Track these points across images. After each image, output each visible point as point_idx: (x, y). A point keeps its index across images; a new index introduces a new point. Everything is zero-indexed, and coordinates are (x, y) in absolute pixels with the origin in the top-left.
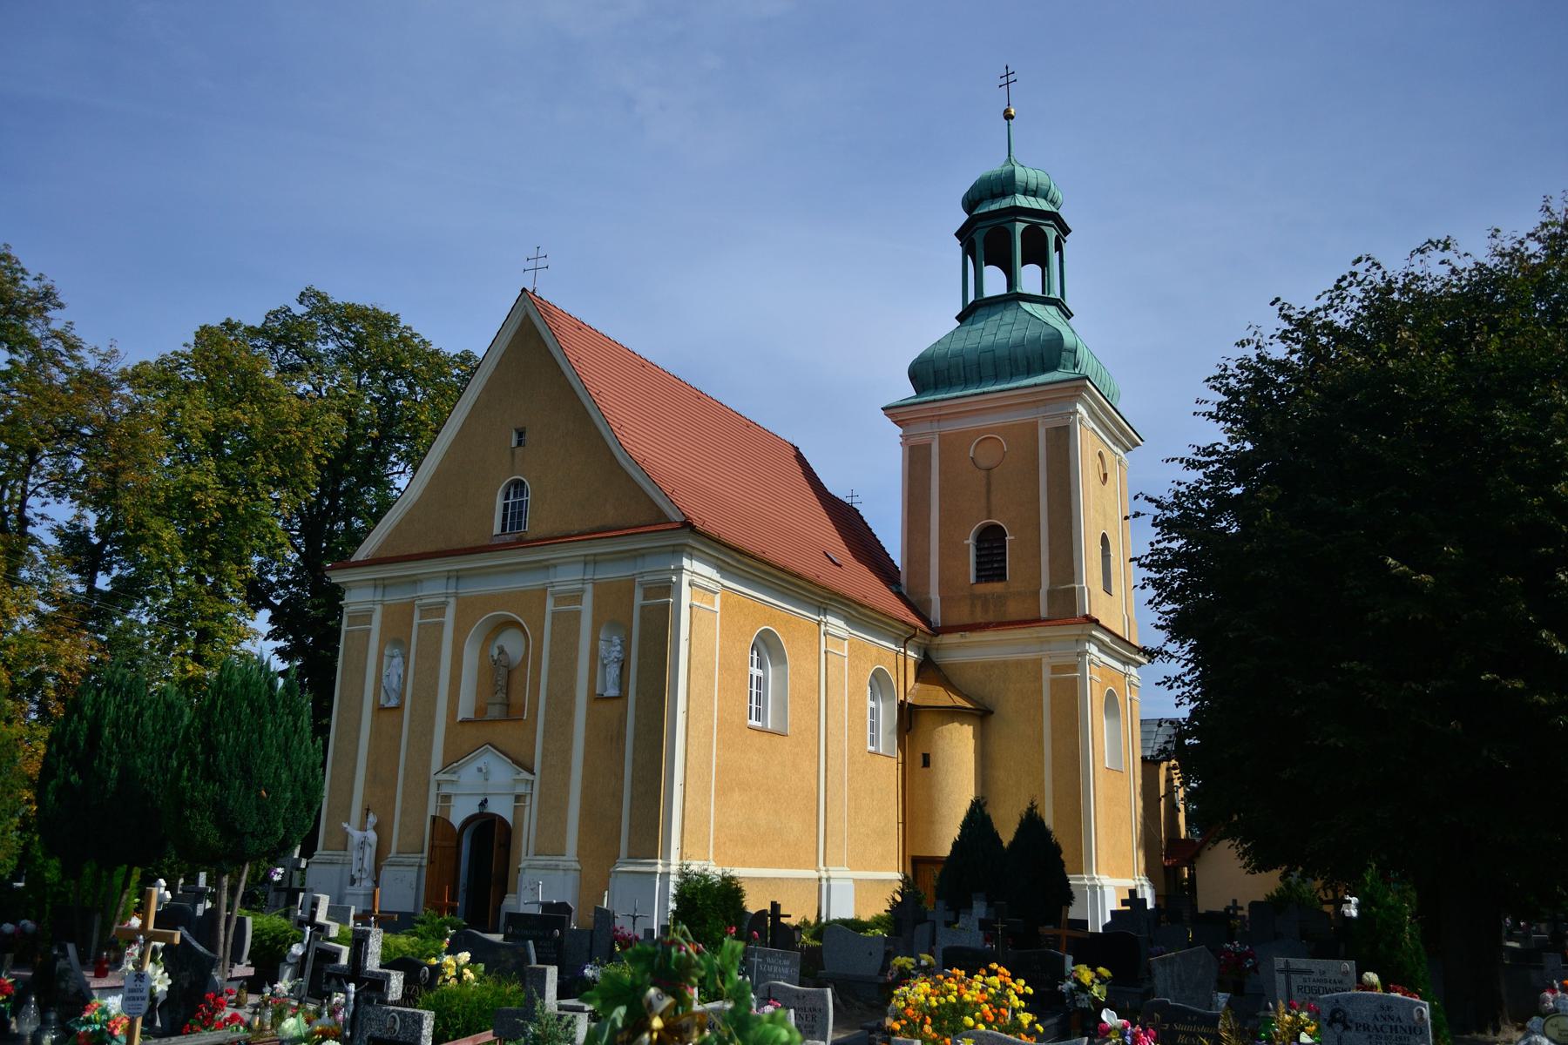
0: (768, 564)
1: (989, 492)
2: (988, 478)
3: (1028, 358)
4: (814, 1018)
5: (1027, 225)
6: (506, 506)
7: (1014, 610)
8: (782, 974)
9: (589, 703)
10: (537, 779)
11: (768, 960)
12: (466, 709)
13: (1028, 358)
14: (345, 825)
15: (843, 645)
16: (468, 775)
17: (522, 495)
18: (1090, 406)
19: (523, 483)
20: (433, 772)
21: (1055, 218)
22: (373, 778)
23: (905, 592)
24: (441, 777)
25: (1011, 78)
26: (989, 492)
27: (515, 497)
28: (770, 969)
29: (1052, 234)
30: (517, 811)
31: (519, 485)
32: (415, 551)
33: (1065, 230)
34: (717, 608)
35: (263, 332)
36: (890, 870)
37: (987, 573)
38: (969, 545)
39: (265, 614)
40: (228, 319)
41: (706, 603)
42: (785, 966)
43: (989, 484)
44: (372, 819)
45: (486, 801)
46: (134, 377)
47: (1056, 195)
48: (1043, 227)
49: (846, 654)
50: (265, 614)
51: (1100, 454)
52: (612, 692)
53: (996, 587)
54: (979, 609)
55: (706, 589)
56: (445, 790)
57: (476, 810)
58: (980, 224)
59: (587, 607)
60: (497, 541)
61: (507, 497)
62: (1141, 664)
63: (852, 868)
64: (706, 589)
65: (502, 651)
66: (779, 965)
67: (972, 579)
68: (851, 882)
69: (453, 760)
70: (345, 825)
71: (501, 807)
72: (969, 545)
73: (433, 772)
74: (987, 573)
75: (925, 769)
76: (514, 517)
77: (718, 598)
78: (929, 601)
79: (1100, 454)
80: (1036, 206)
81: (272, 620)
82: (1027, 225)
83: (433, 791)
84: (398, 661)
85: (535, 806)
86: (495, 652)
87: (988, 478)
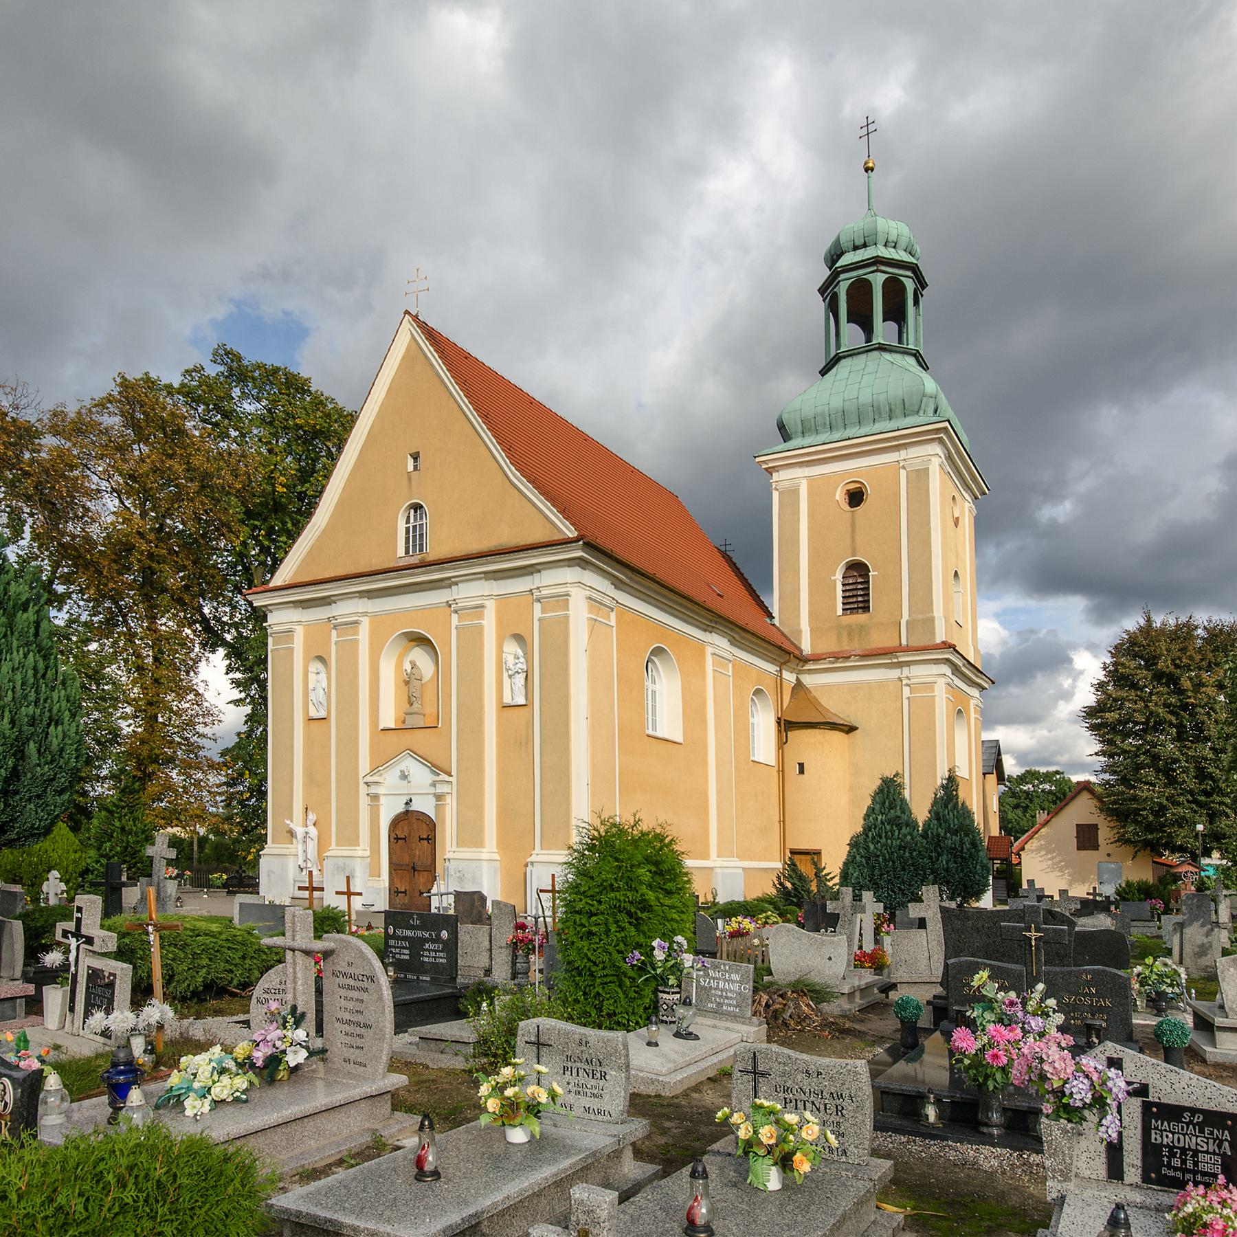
0: (658, 583)
1: (853, 531)
2: (853, 516)
3: (890, 404)
4: (839, 1110)
5: (887, 276)
6: (407, 530)
7: (879, 640)
8: (731, 991)
9: (498, 713)
10: (453, 779)
11: (711, 973)
12: (388, 718)
13: (890, 404)
14: (288, 822)
15: (727, 665)
16: (390, 779)
17: (421, 518)
18: (947, 449)
19: (421, 507)
20: (361, 775)
21: (914, 269)
22: (310, 779)
23: (778, 624)
24: (368, 779)
25: (871, 128)
26: (853, 531)
27: (415, 520)
28: (714, 984)
29: (910, 285)
30: (439, 808)
31: (417, 507)
32: (328, 576)
33: (921, 283)
34: (613, 623)
35: (185, 391)
36: (773, 860)
37: (852, 606)
38: (835, 581)
39: (221, 652)
40: (146, 374)
41: (602, 617)
42: (733, 982)
43: (853, 524)
44: (312, 817)
45: (411, 800)
46: (59, 424)
47: (915, 247)
48: (901, 278)
49: (730, 674)
50: (221, 652)
51: (954, 498)
52: (522, 701)
53: (861, 618)
54: (845, 638)
55: (601, 604)
56: (373, 790)
57: (401, 808)
58: (842, 276)
59: (489, 622)
60: (401, 563)
61: (408, 521)
62: (984, 688)
63: (741, 858)
64: (601, 604)
65: (414, 666)
66: (725, 980)
67: (840, 612)
68: (741, 870)
69: (380, 764)
70: (288, 822)
71: (424, 805)
72: (835, 581)
73: (361, 775)
74: (852, 606)
75: (801, 776)
76: (415, 538)
77: (613, 615)
78: (799, 632)
79: (954, 498)
80: (896, 257)
81: (228, 656)
82: (887, 276)
83: (363, 790)
84: (323, 676)
85: (455, 804)
86: (408, 667)
87: (853, 516)
